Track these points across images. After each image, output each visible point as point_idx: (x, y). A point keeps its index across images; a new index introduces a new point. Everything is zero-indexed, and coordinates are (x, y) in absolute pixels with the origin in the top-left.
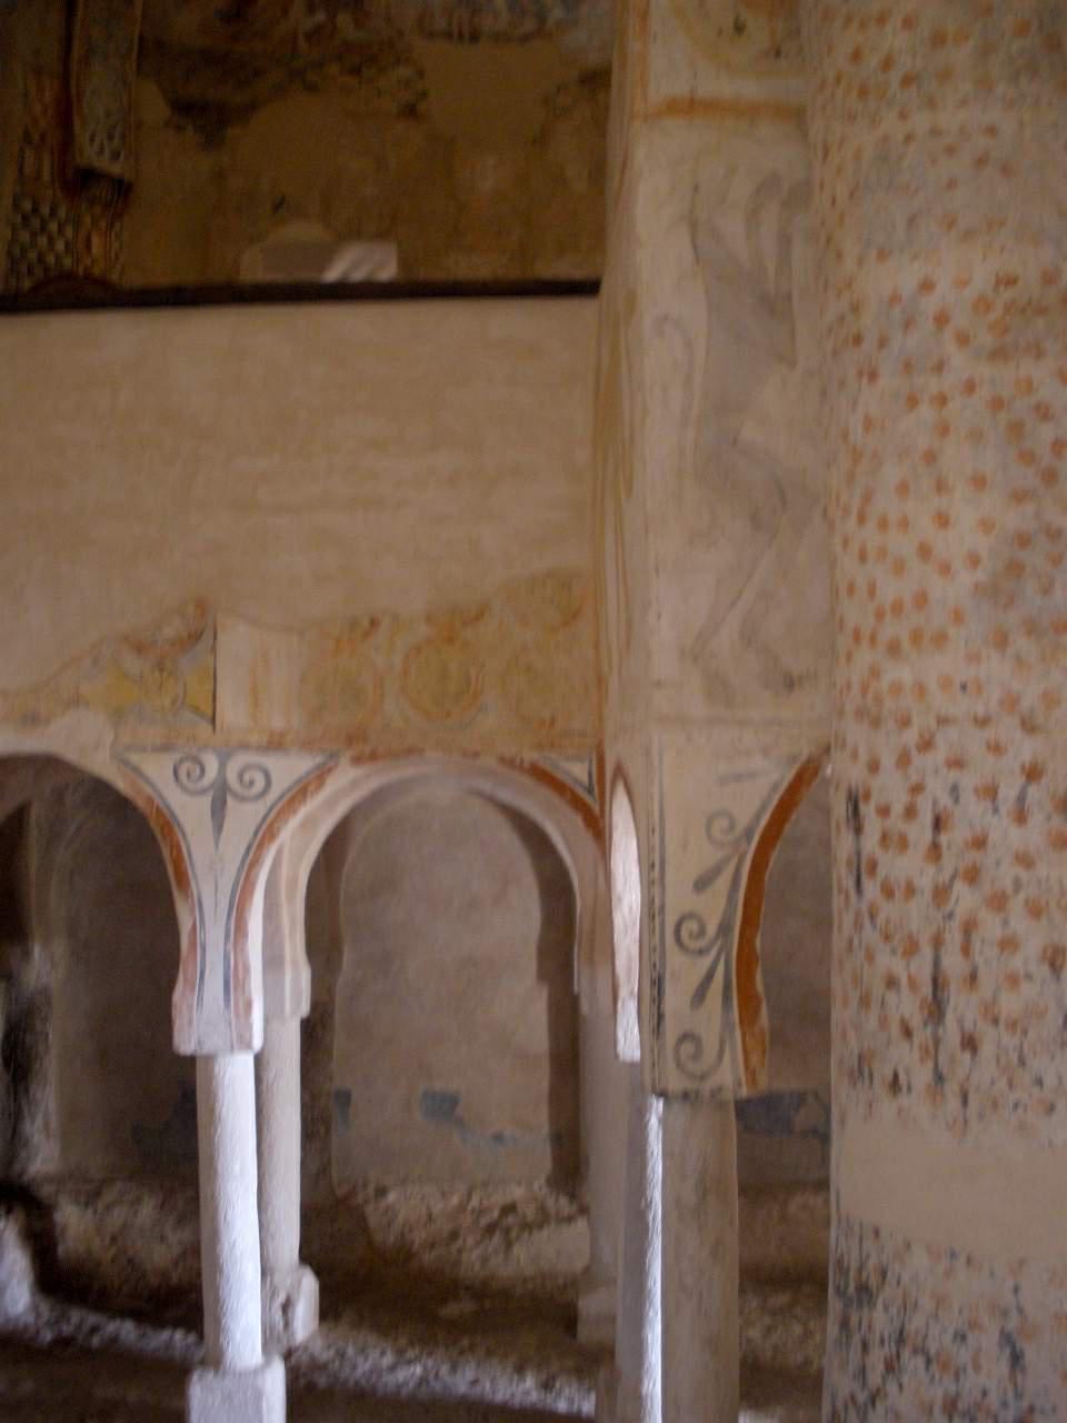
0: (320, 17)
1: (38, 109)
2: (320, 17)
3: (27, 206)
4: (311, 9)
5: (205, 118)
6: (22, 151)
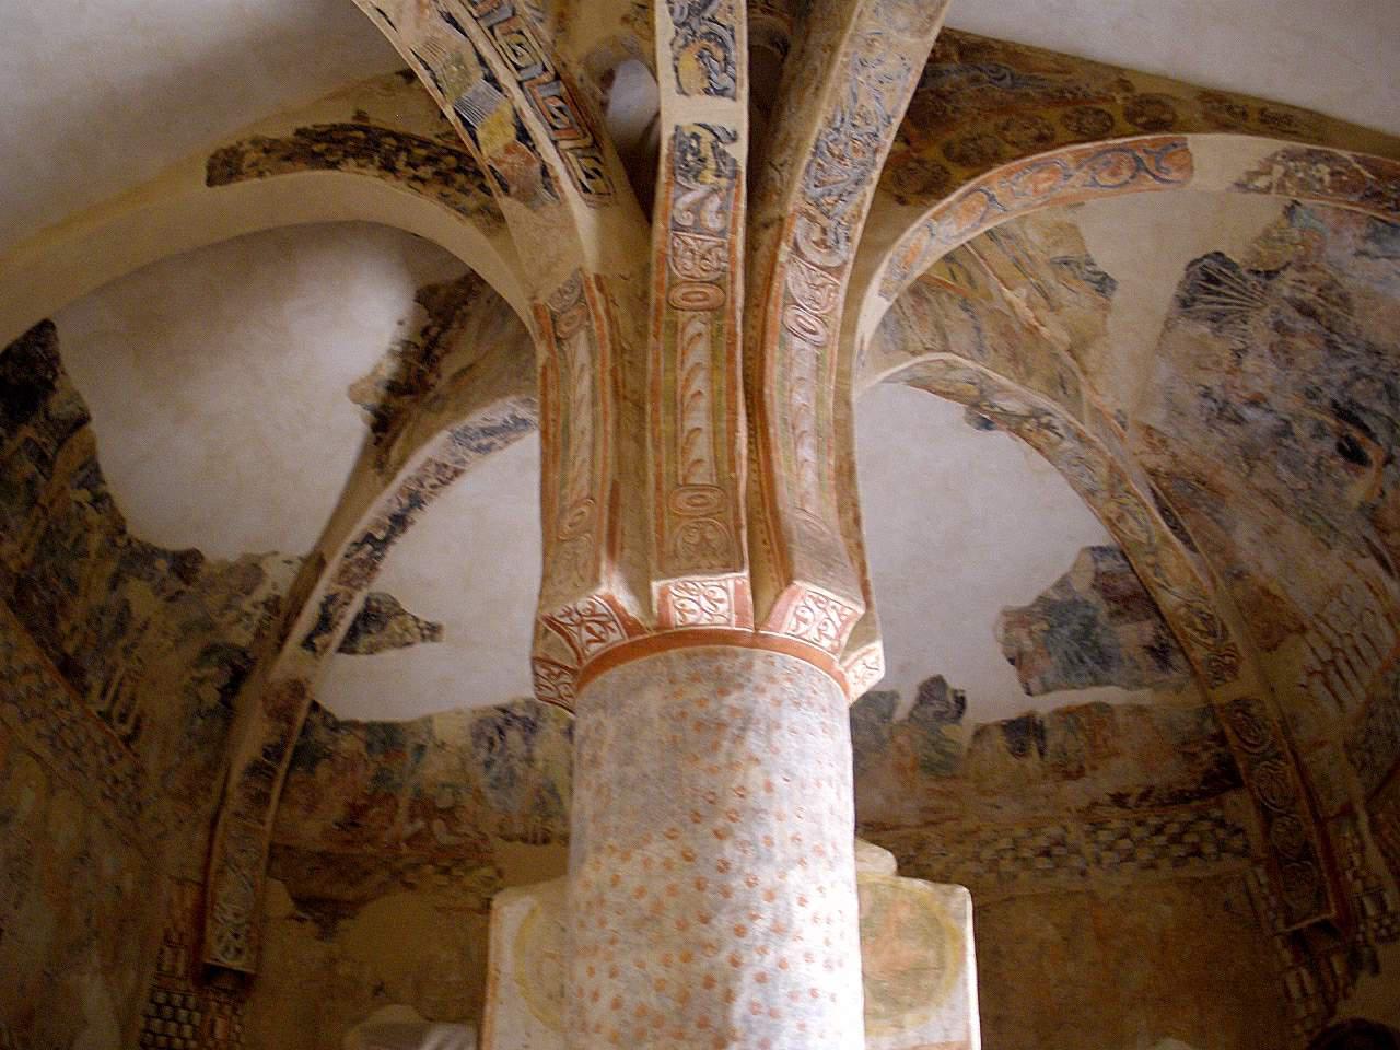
0: (420, 824)
1: (178, 913)
2: (420, 824)
3: (161, 998)
4: (412, 818)
5: (323, 911)
6: (162, 952)
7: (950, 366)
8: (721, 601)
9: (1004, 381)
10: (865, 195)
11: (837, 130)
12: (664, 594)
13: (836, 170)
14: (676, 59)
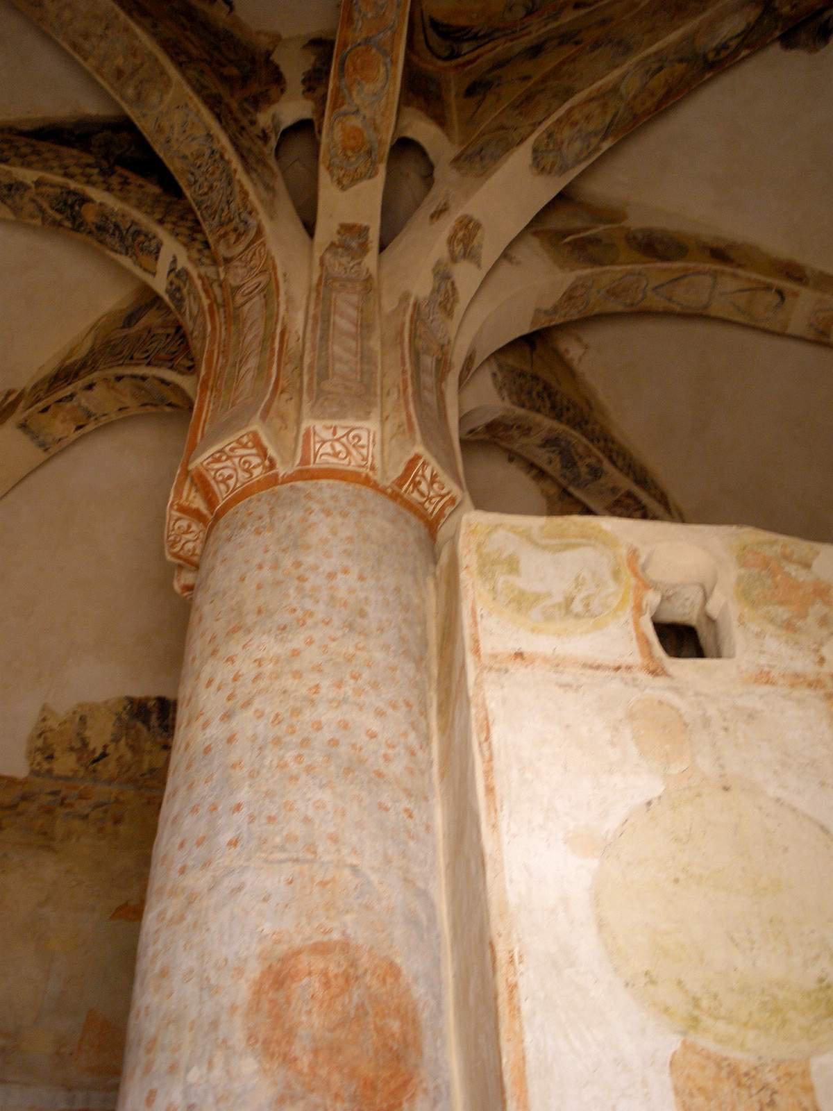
7: (615, 89)
8: (189, 527)
9: (674, 37)
10: (239, 181)
11: (196, 182)
12: (176, 555)
13: (215, 196)
14: (141, 266)
